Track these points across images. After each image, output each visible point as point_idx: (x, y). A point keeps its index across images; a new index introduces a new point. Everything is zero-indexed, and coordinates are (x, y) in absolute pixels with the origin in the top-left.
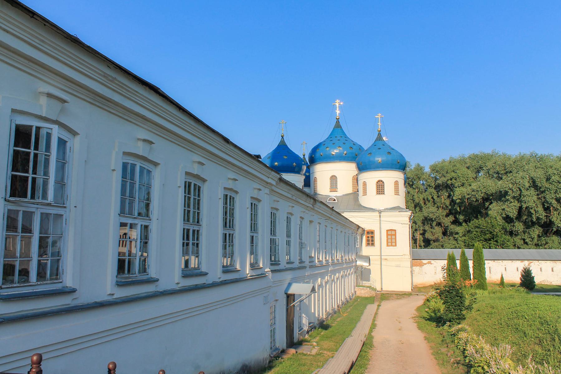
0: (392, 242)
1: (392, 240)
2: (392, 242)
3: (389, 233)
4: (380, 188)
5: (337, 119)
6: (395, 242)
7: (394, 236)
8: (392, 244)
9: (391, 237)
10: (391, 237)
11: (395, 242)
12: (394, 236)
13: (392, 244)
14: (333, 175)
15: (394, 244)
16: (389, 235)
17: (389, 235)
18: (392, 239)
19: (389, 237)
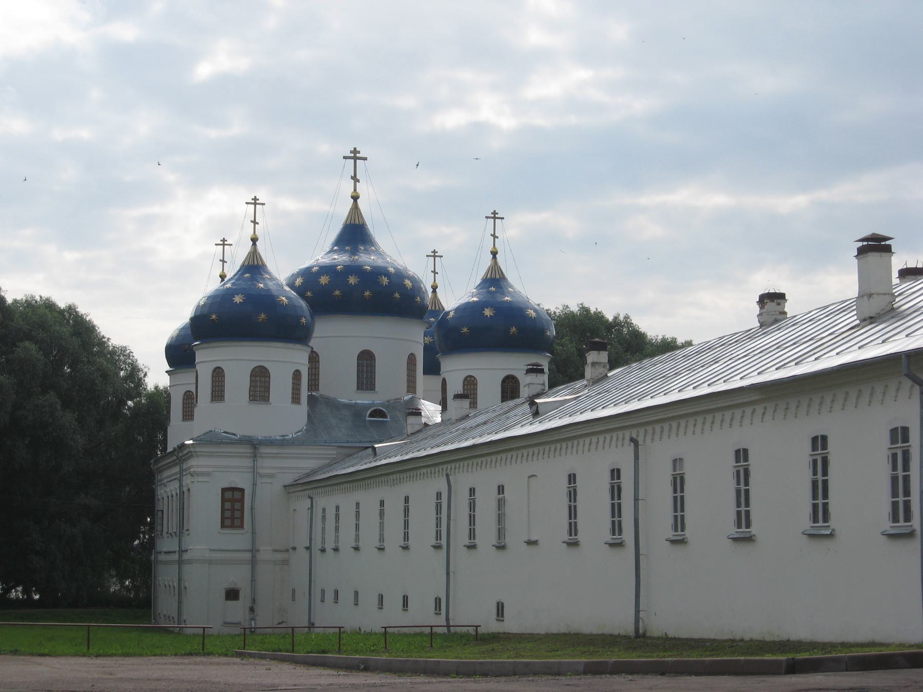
0: (233, 518)
2: (233, 518)
3: (228, 495)
9: (233, 506)
10: (233, 506)
15: (237, 522)
18: (233, 510)
19: (228, 505)
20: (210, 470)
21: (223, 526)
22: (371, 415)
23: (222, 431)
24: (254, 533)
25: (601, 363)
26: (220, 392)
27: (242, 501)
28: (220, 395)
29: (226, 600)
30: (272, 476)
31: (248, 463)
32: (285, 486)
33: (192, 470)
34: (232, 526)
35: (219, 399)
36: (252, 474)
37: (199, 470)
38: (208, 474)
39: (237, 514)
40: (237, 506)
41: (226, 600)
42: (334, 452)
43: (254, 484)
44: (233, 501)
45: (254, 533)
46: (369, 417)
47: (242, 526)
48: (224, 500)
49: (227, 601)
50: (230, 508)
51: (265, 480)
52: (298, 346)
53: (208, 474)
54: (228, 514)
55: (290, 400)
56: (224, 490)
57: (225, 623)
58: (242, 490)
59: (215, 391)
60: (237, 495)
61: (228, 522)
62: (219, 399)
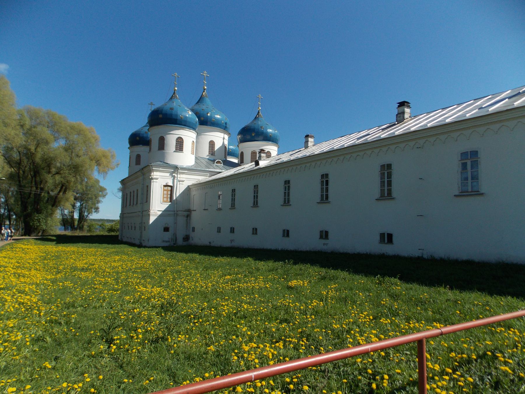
4: (180, 145)
10: (167, 193)
18: (167, 194)
19: (165, 192)
20: (158, 177)
22: (217, 163)
30: (183, 181)
33: (151, 177)
37: (154, 177)
38: (157, 179)
44: (167, 190)
48: (164, 190)
50: (166, 193)
51: (181, 183)
53: (157, 179)
54: (165, 196)
56: (165, 186)
57: (163, 241)
61: (165, 199)
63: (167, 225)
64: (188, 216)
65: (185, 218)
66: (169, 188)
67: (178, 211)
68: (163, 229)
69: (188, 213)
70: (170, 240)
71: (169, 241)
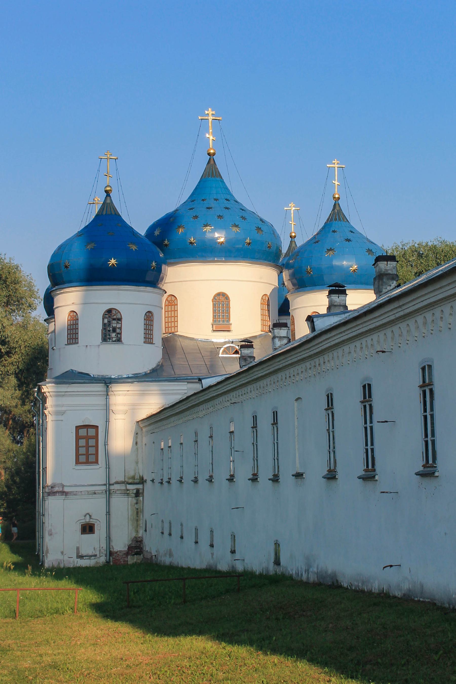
0: (87, 455)
1: (87, 450)
2: (87, 455)
3: (83, 432)
5: (209, 154)
6: (94, 453)
7: (94, 440)
8: (87, 458)
9: (87, 443)
10: (87, 443)
11: (94, 453)
12: (94, 440)
13: (87, 458)
14: (226, 294)
15: (92, 458)
16: (82, 438)
17: (82, 438)
18: (87, 447)
19: (82, 442)
20: (64, 409)
21: (78, 462)
23: (77, 372)
24: (108, 467)
25: (389, 274)
26: (74, 335)
27: (96, 437)
28: (74, 337)
29: (81, 534)
31: (101, 401)
32: (138, 422)
34: (87, 462)
35: (74, 342)
36: (106, 410)
39: (92, 450)
40: (92, 442)
41: (81, 534)
42: (185, 388)
43: (107, 421)
44: (87, 438)
45: (108, 467)
46: (222, 354)
47: (96, 462)
48: (78, 438)
49: (82, 535)
52: (149, 289)
54: (82, 451)
55: (143, 340)
56: (78, 428)
58: (96, 427)
59: (70, 334)
60: (92, 432)
61: (82, 459)
62: (74, 342)
63: (88, 516)
64: (138, 494)
65: (132, 500)
66: (92, 432)
67: (113, 485)
68: (79, 528)
69: (140, 486)
70: (98, 553)
71: (95, 556)
